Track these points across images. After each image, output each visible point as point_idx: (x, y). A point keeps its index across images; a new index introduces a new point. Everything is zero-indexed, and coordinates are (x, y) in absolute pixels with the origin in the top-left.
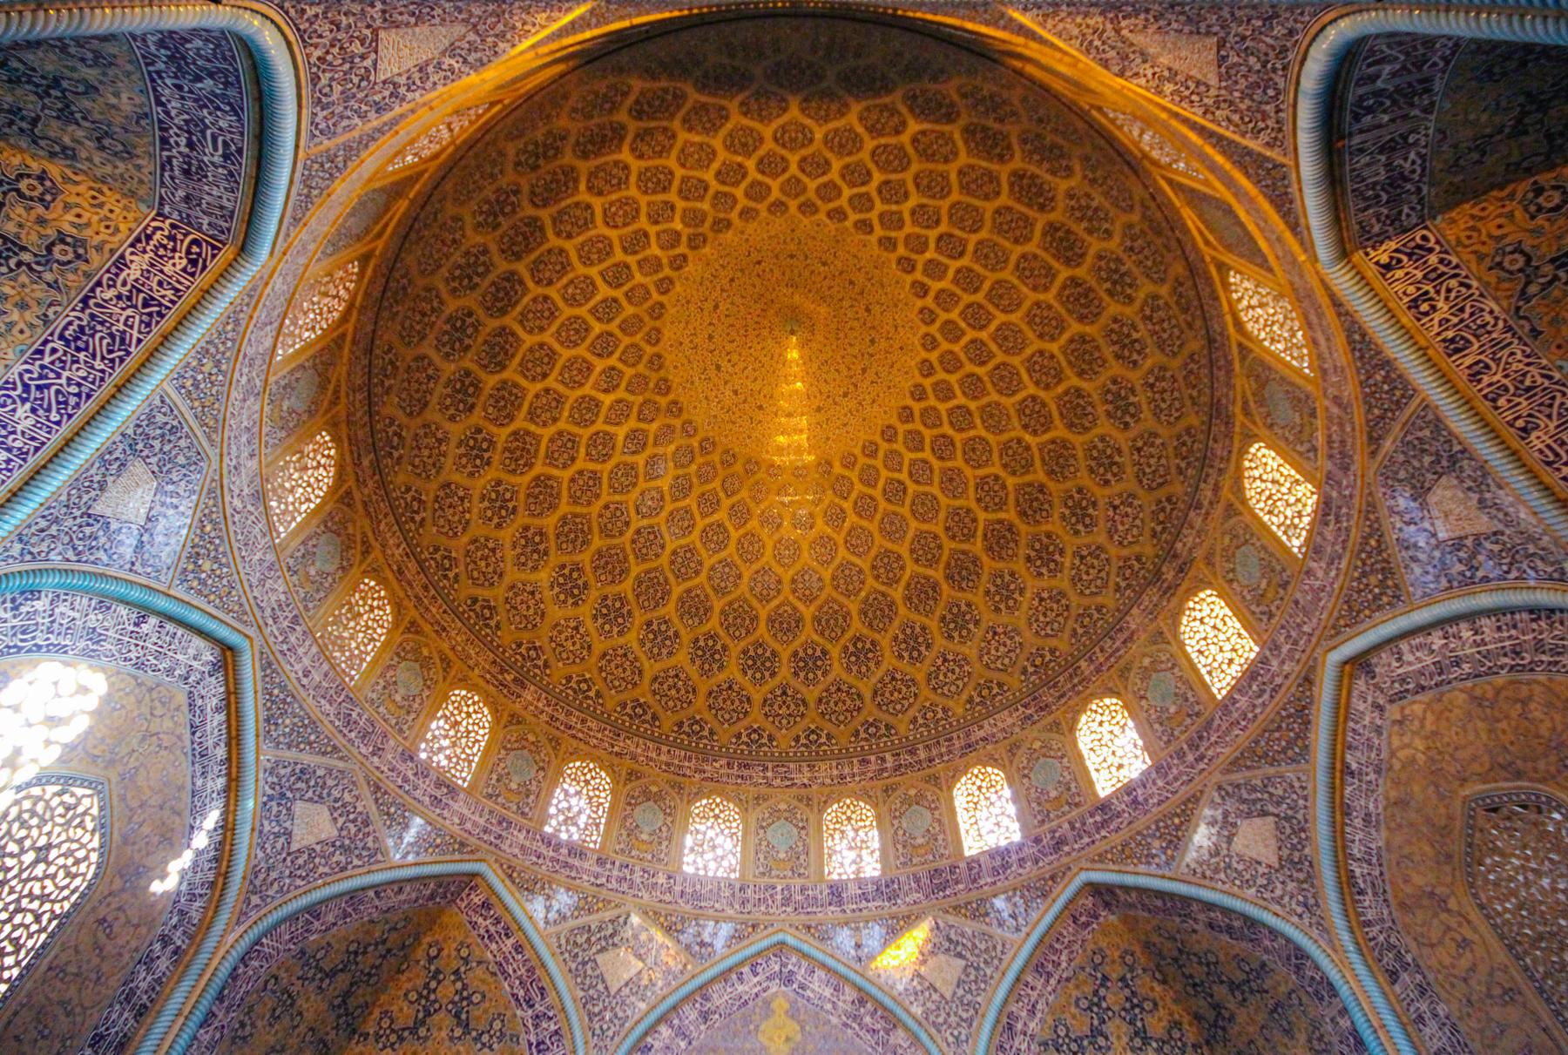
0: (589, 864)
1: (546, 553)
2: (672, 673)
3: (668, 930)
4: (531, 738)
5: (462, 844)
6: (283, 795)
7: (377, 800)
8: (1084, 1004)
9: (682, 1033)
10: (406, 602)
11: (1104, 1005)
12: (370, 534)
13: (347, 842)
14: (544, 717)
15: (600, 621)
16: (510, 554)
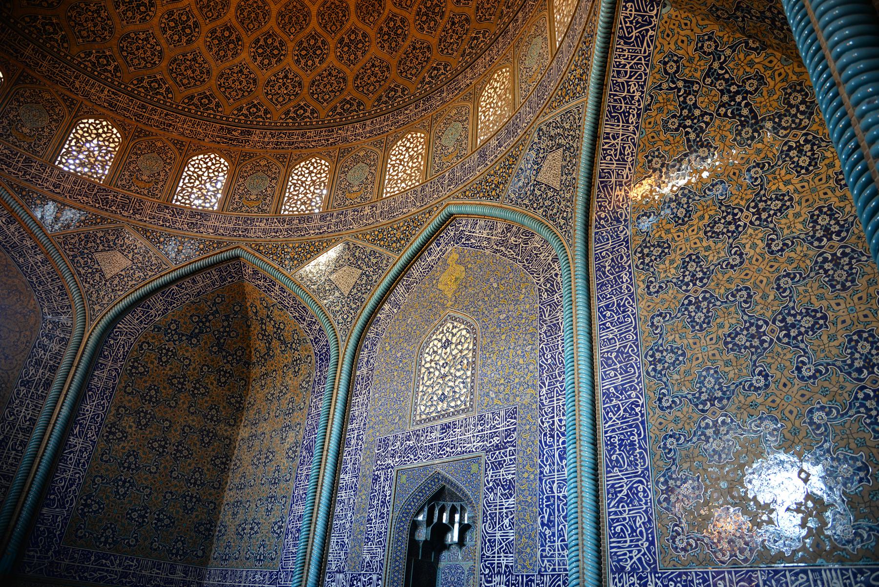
0: (316, 223)
1: (239, 39)
2: (368, 66)
3: (373, 242)
4: (263, 163)
5: (219, 243)
6: (82, 253)
7: (148, 238)
8: (674, 123)
9: (397, 305)
10: (127, 121)
11: (697, 113)
12: (68, 93)
13: (140, 265)
14: (271, 146)
15: (303, 62)
16: (209, 56)
